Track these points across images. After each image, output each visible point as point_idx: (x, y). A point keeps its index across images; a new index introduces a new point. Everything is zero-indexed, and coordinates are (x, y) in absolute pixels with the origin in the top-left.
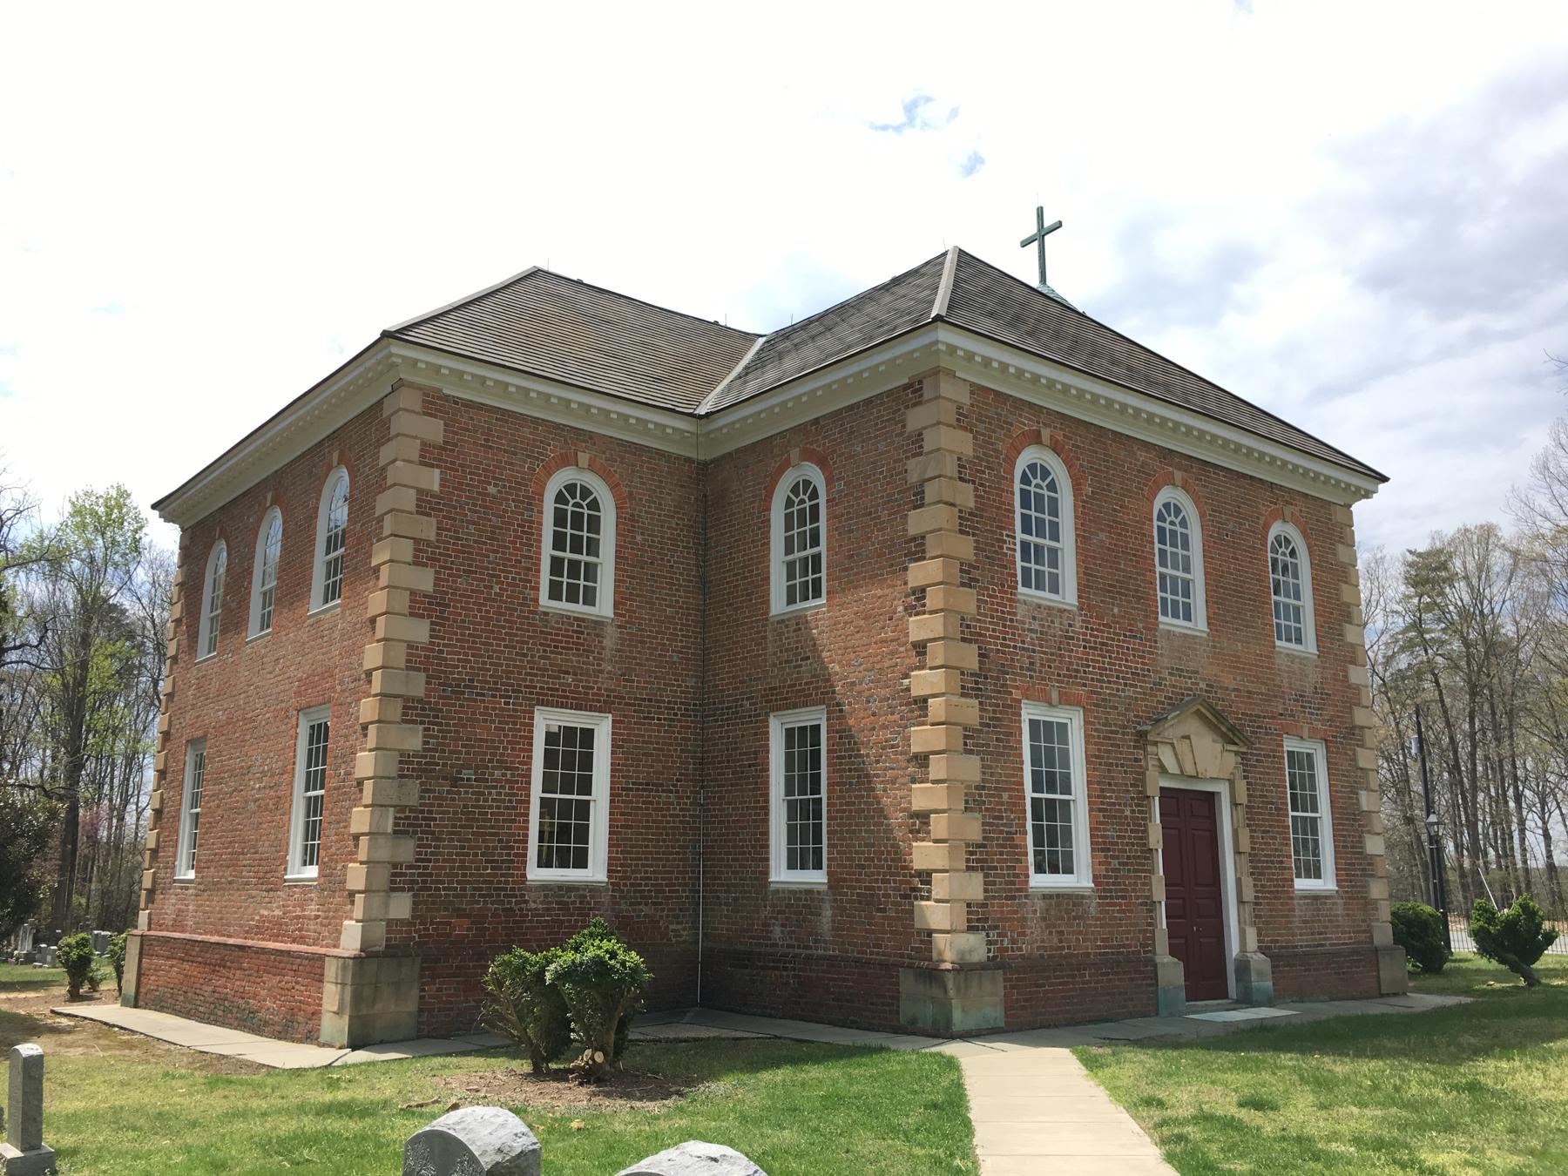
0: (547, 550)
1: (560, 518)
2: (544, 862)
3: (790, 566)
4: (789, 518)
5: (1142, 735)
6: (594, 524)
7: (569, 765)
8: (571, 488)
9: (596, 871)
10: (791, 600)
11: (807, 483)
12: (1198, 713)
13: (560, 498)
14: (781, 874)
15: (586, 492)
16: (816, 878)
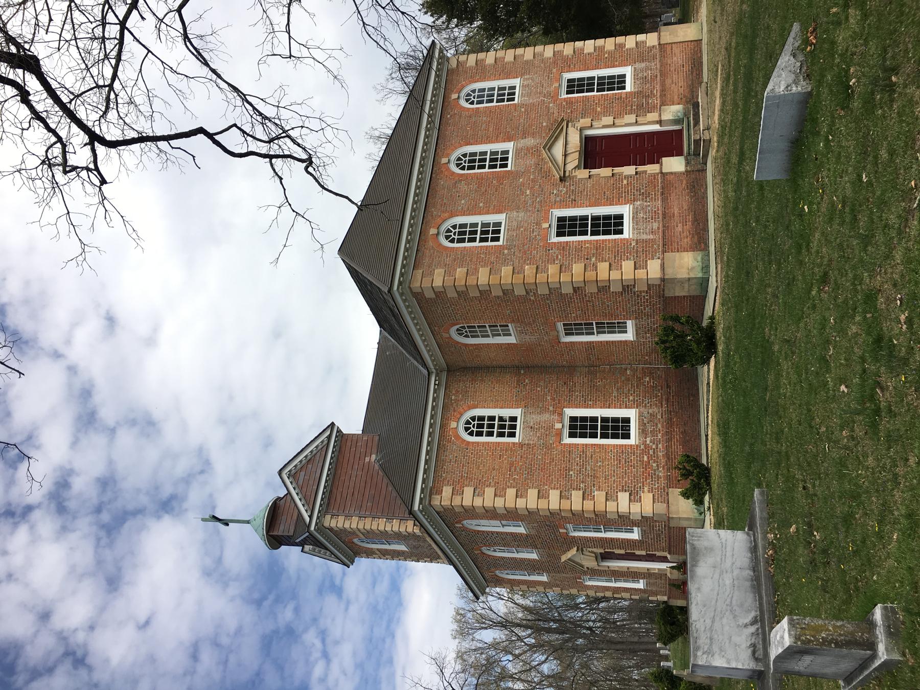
0: (494, 439)
1: (479, 434)
2: (627, 436)
3: (494, 335)
4: (472, 336)
5: (563, 179)
6: (481, 418)
7: (585, 427)
8: (467, 429)
9: (631, 414)
10: (510, 335)
11: (458, 330)
12: (549, 149)
13: (471, 434)
14: (629, 335)
15: (468, 423)
16: (630, 324)
